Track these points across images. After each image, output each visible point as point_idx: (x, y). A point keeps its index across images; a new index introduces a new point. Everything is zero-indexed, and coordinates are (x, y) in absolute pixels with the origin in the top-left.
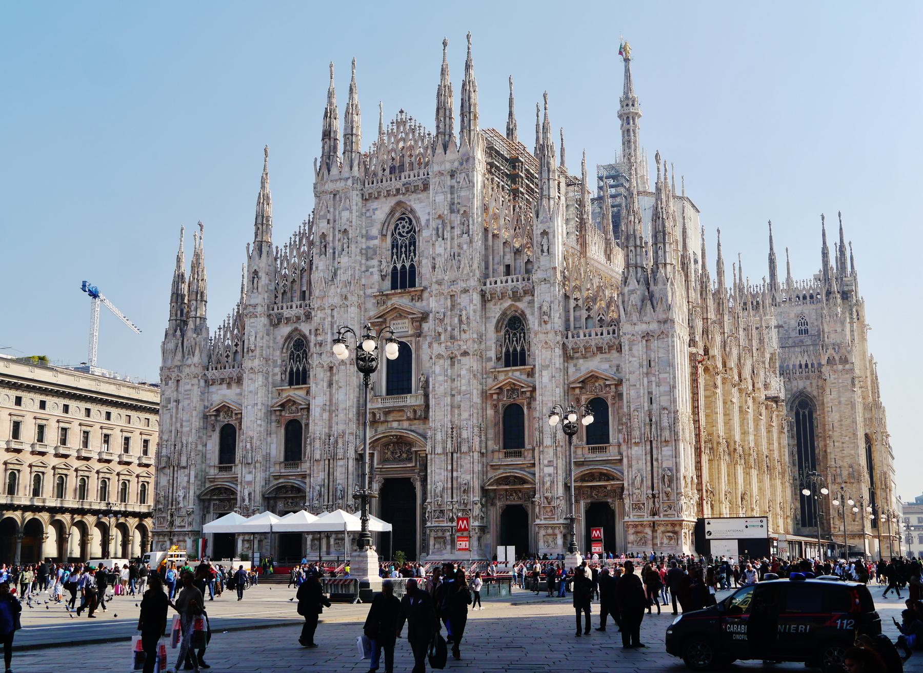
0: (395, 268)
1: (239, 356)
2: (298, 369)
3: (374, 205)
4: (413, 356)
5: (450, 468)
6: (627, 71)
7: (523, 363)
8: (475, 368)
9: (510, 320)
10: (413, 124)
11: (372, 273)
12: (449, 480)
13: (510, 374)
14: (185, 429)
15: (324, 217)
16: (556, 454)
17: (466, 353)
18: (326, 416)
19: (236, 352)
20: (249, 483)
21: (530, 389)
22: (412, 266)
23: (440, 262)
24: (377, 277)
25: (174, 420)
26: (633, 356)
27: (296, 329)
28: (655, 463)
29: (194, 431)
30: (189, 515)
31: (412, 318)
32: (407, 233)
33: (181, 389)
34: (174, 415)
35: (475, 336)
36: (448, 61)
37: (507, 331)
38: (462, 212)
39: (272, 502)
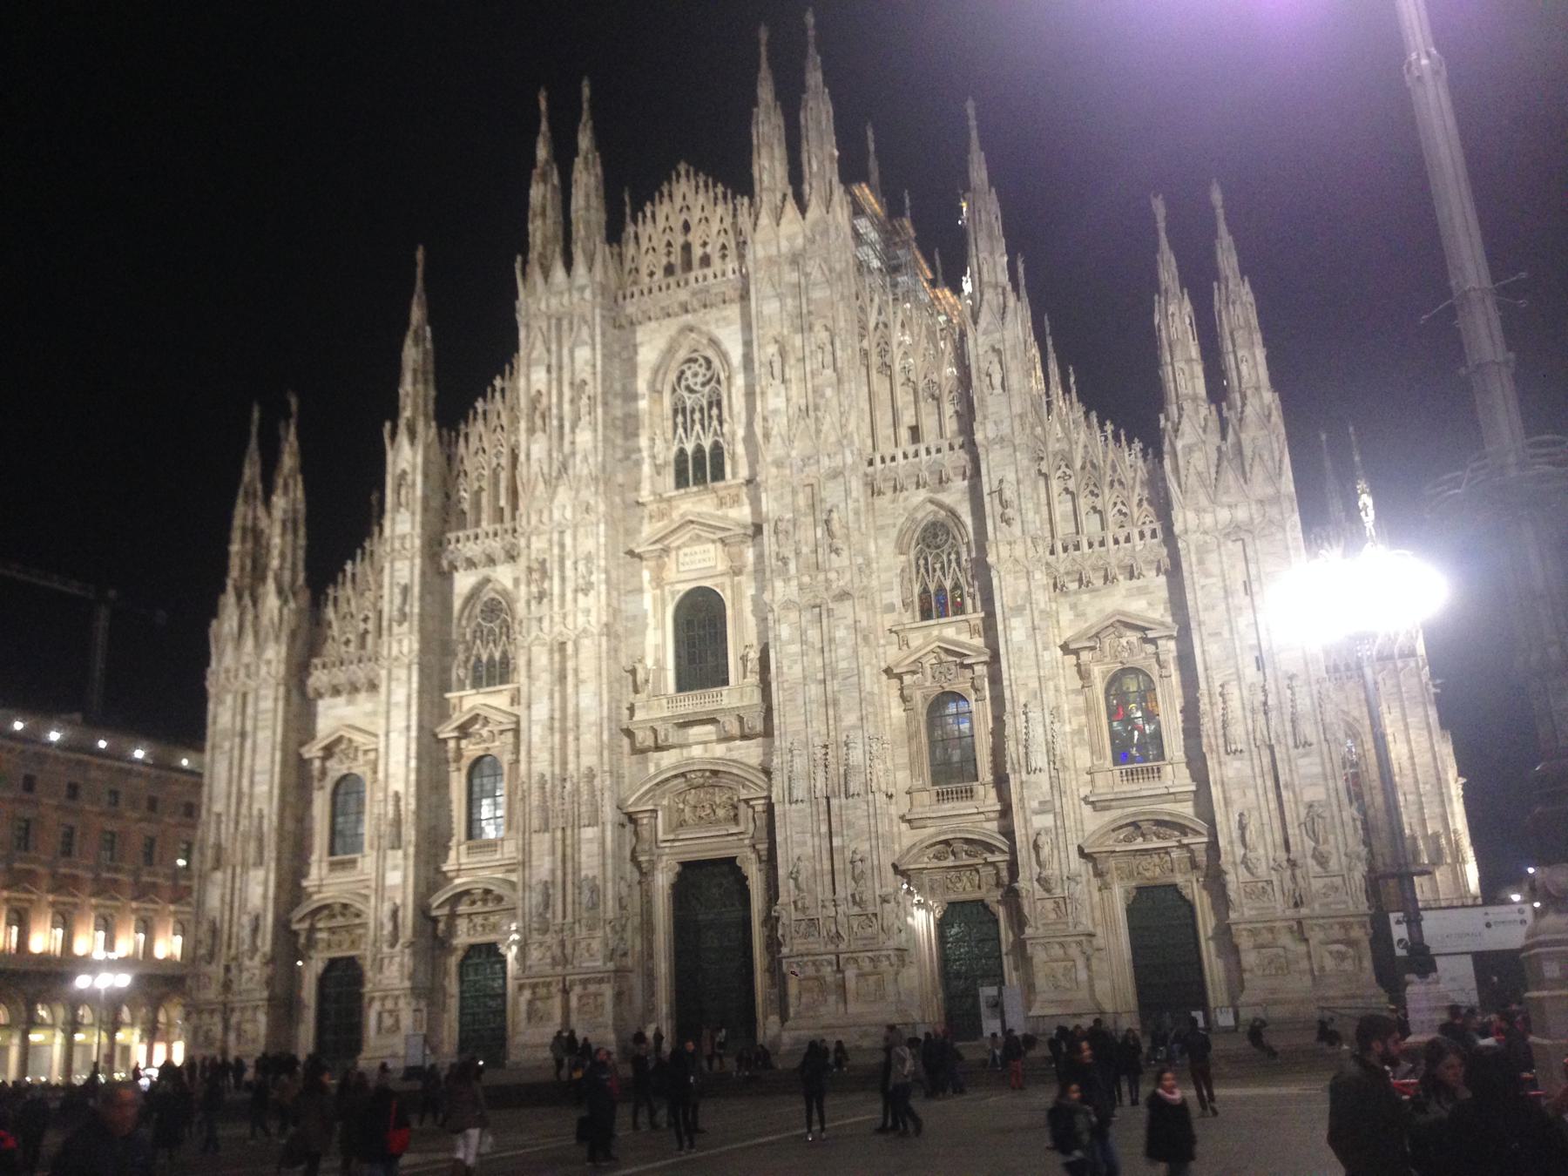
1: (370, 639)
2: (491, 658)
4: (729, 612)
5: (824, 829)
7: (960, 609)
8: (864, 623)
9: (925, 530)
12: (826, 855)
13: (935, 632)
14: (262, 789)
15: (538, 362)
16: (1056, 786)
17: (844, 596)
20: (394, 887)
21: (985, 658)
22: (717, 447)
23: (779, 426)
24: (646, 469)
25: (235, 772)
26: (1208, 575)
27: (487, 580)
28: (1284, 793)
29: (276, 792)
31: (722, 540)
33: (250, 711)
34: (236, 762)
35: (860, 560)
37: (921, 551)
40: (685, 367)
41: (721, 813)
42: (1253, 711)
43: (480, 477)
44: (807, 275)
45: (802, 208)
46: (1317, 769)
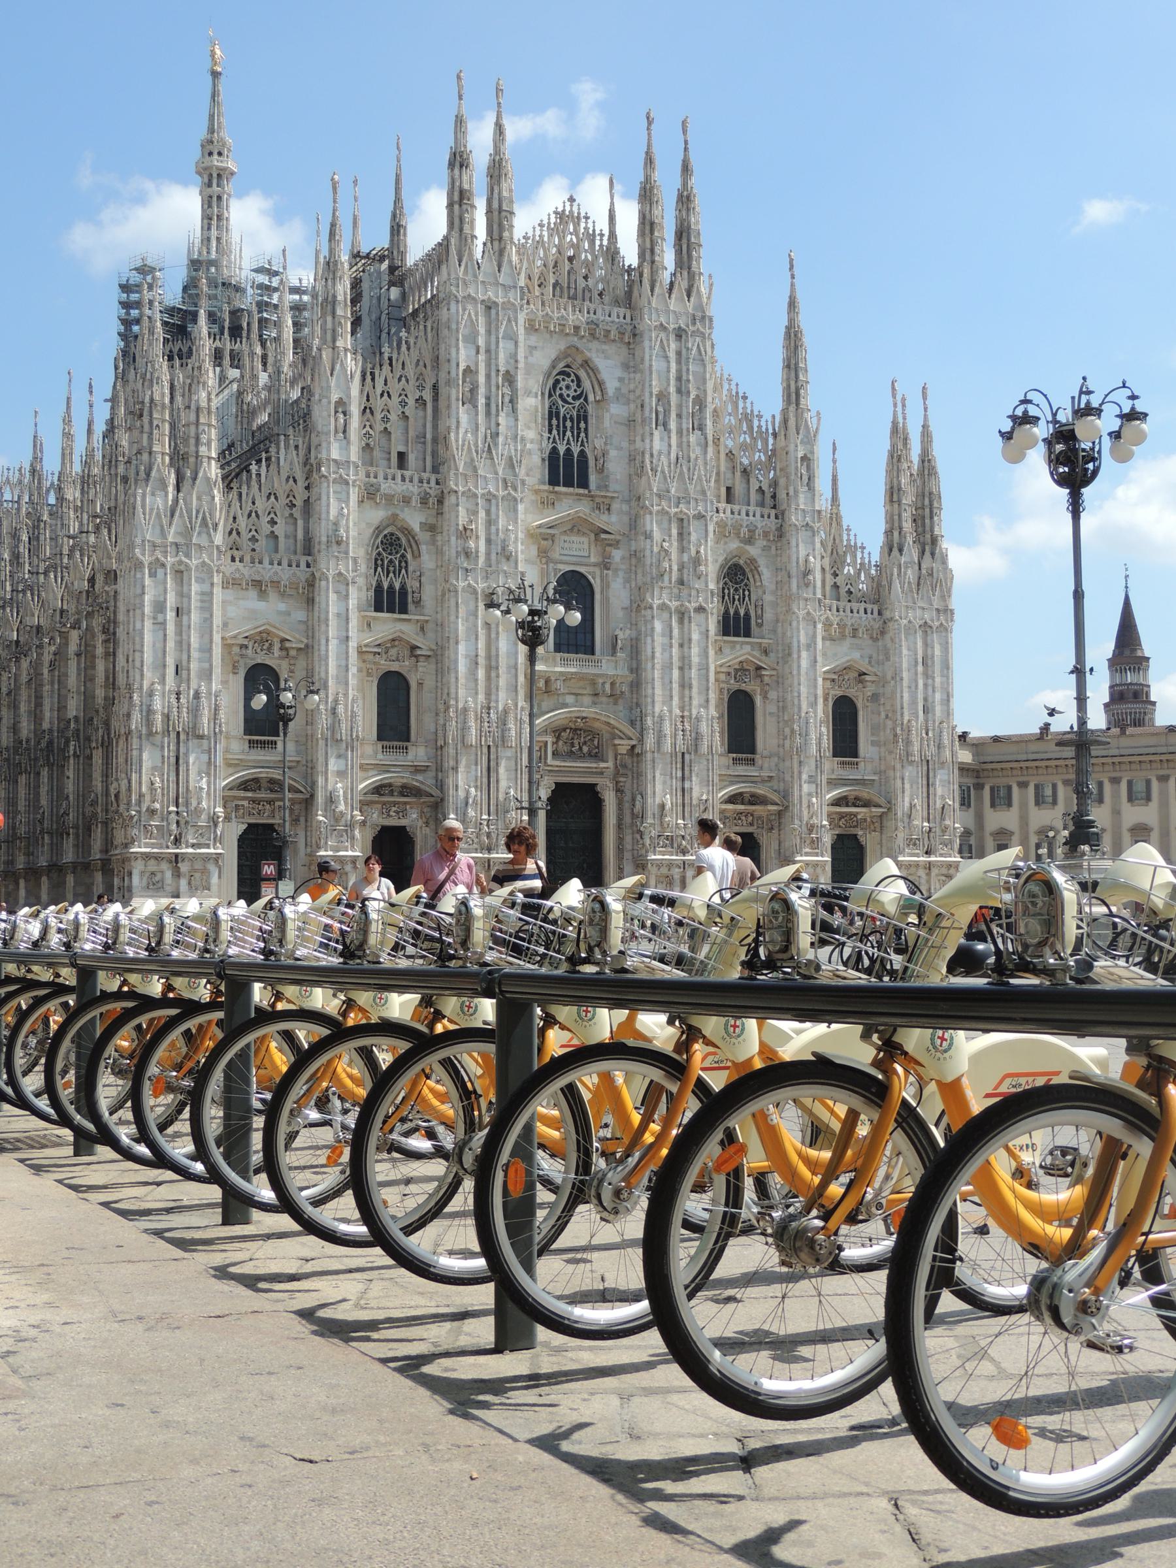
0: (554, 450)
2: (391, 587)
3: (534, 340)
4: (597, 597)
5: (679, 774)
6: (214, 95)
7: (748, 634)
10: (590, 225)
11: (530, 452)
12: (679, 793)
13: (738, 647)
17: (700, 609)
18: (481, 673)
19: (272, 532)
24: (536, 459)
30: (216, 825)
32: (574, 398)
36: (654, 150)
37: (725, 583)
38: (692, 396)
39: (365, 807)
40: (560, 377)
41: (585, 749)
42: (922, 739)
43: (385, 419)
44: (688, 349)
45: (689, 296)
46: (946, 777)
